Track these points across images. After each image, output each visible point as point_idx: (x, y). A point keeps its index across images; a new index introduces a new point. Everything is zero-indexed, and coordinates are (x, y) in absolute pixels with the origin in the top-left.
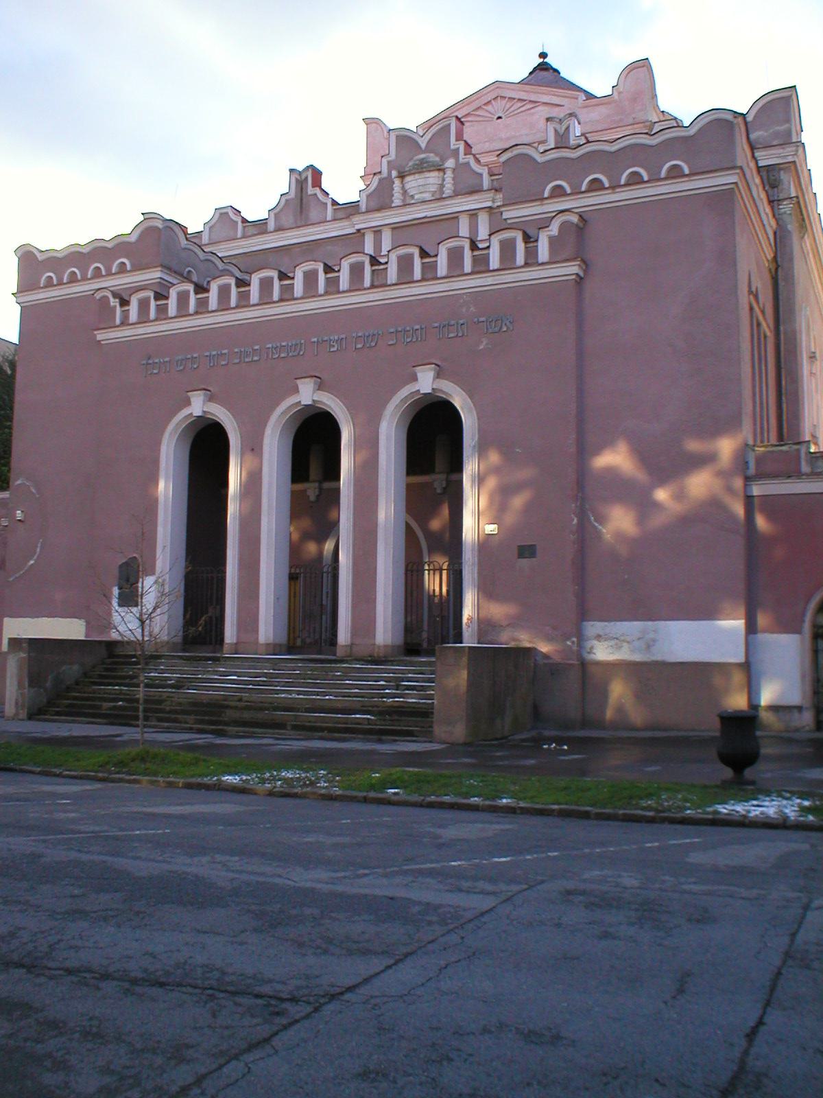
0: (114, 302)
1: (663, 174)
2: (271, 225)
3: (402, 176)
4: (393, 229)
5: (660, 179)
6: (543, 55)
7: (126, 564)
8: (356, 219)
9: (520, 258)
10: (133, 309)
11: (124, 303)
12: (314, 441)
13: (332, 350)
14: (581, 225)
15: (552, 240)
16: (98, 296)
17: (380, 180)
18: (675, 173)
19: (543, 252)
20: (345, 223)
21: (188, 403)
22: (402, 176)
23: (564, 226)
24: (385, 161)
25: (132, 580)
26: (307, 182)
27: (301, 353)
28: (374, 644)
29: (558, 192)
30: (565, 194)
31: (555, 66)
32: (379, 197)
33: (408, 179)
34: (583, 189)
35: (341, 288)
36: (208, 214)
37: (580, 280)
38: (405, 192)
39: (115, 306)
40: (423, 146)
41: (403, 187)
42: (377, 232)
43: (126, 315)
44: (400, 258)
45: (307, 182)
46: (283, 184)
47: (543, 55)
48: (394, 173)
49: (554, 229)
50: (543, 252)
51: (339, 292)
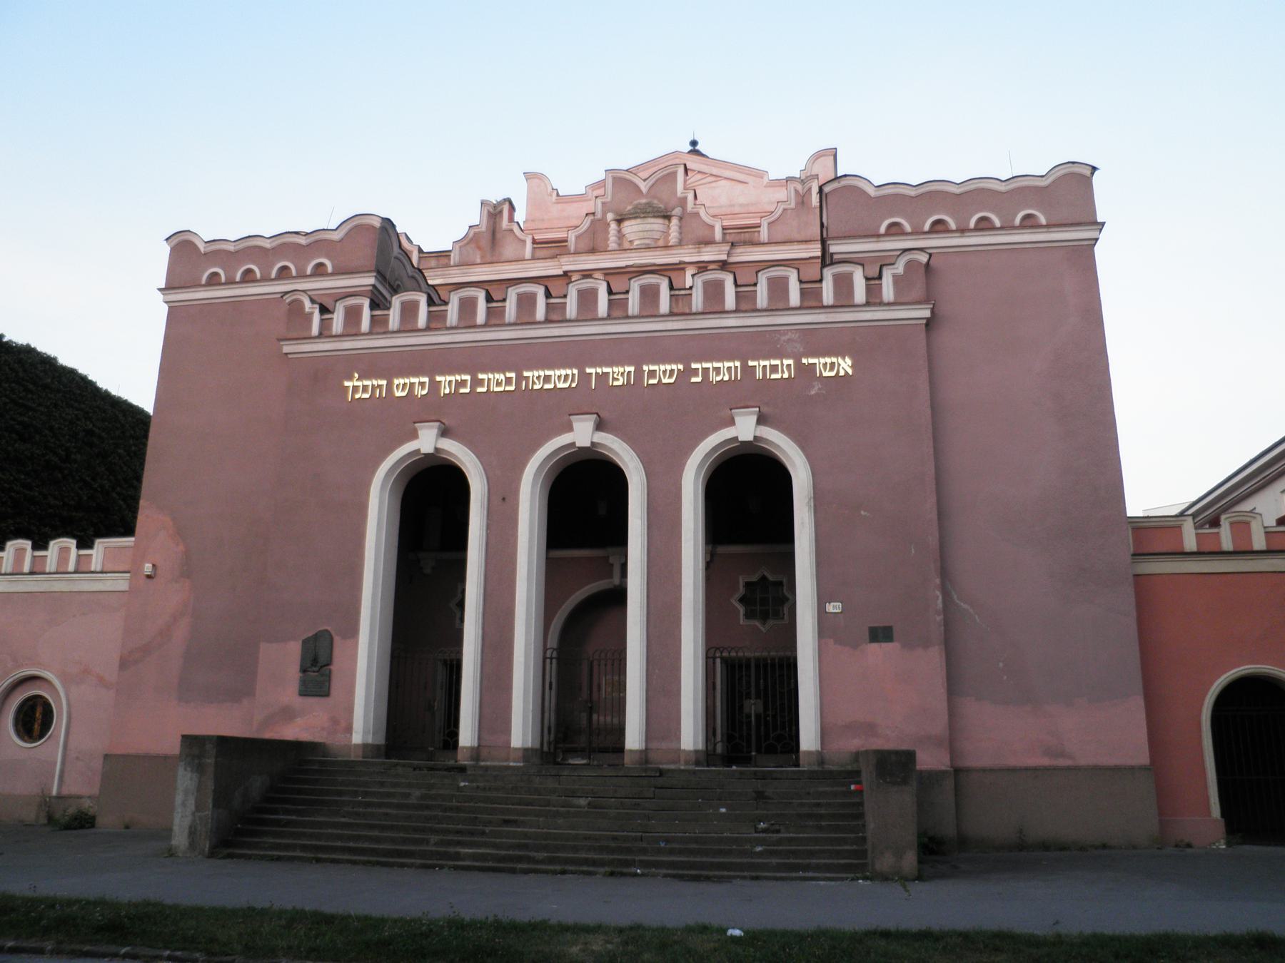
2: (454, 258)
3: (619, 221)
4: (606, 274)
5: (1014, 228)
6: (694, 143)
7: (316, 637)
8: (564, 259)
13: (616, 383)
15: (897, 279)
16: (288, 299)
17: (592, 222)
18: (1029, 223)
19: (888, 292)
20: (550, 263)
21: (414, 435)
22: (619, 221)
23: (909, 265)
24: (599, 201)
25: (322, 660)
27: (574, 385)
28: (679, 749)
30: (904, 233)
33: (626, 223)
35: (630, 313)
38: (621, 236)
39: (312, 314)
40: (644, 190)
41: (619, 231)
43: (326, 325)
44: (706, 284)
46: (474, 216)
47: (694, 143)
48: (610, 216)
49: (900, 268)
50: (888, 292)
51: (628, 317)
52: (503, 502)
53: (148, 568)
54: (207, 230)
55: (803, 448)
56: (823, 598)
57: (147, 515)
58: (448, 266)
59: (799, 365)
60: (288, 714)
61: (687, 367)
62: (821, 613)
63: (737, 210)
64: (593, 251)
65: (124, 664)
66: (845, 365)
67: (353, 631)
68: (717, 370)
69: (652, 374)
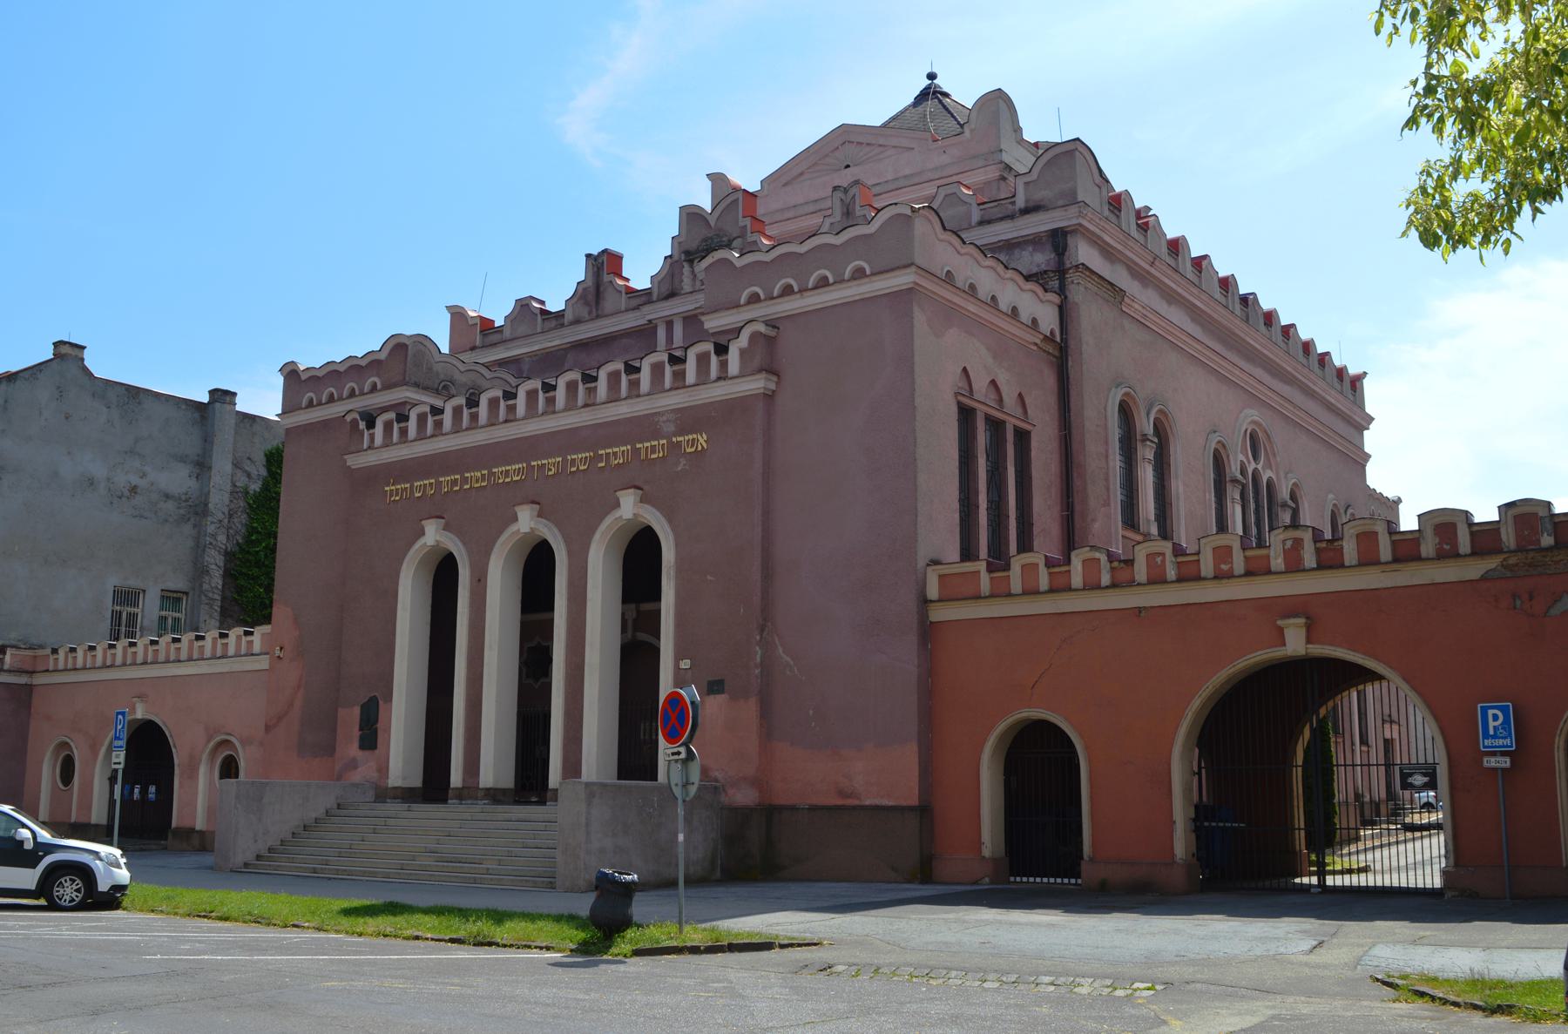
0: (362, 425)
1: (847, 275)
2: (569, 317)
3: (691, 262)
6: (932, 76)
8: (646, 309)
9: (714, 373)
10: (412, 425)
11: (371, 424)
12: (537, 569)
14: (772, 333)
15: (743, 352)
16: (349, 418)
19: (734, 365)
20: (637, 313)
21: (422, 533)
22: (691, 262)
23: (755, 337)
26: (605, 265)
29: (754, 299)
31: (945, 89)
32: (669, 284)
34: (810, 285)
36: (509, 307)
37: (769, 397)
42: (669, 325)
45: (605, 265)
46: (578, 272)
47: (932, 76)
49: (743, 340)
50: (734, 365)
52: (480, 581)
53: (278, 653)
54: (311, 358)
55: (670, 521)
56: (678, 657)
57: (278, 612)
58: (562, 325)
59: (670, 443)
60: (353, 765)
61: (596, 453)
62: (677, 668)
63: (902, 183)
64: (672, 295)
65: (268, 728)
66: (702, 440)
67: (389, 697)
68: (615, 454)
69: (573, 460)
